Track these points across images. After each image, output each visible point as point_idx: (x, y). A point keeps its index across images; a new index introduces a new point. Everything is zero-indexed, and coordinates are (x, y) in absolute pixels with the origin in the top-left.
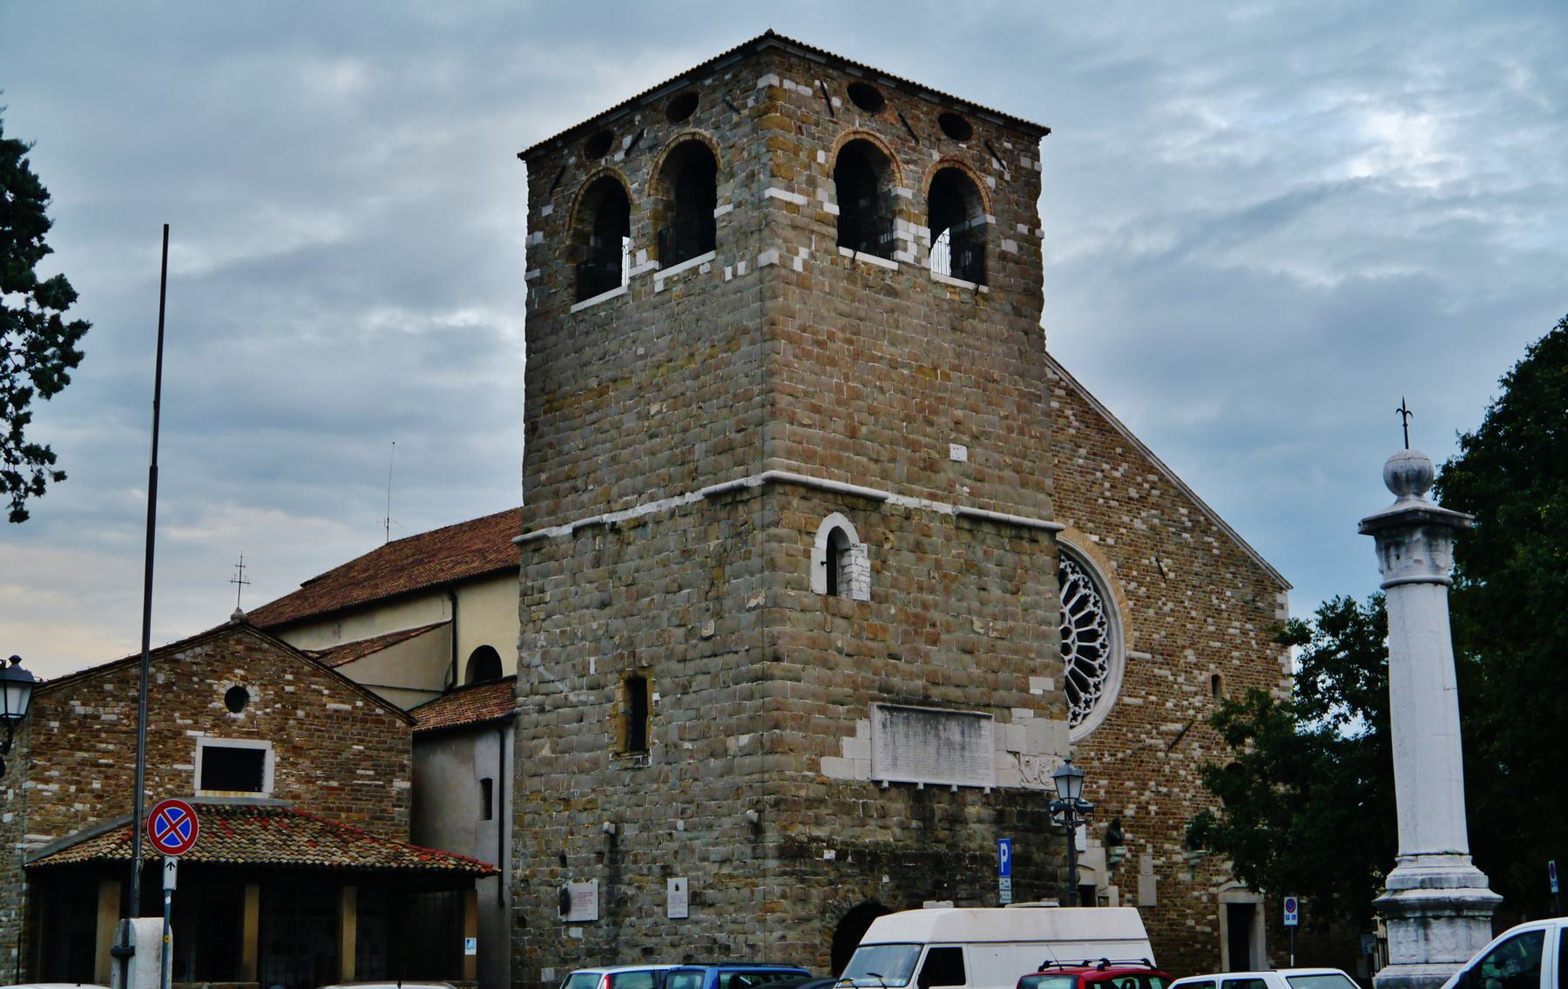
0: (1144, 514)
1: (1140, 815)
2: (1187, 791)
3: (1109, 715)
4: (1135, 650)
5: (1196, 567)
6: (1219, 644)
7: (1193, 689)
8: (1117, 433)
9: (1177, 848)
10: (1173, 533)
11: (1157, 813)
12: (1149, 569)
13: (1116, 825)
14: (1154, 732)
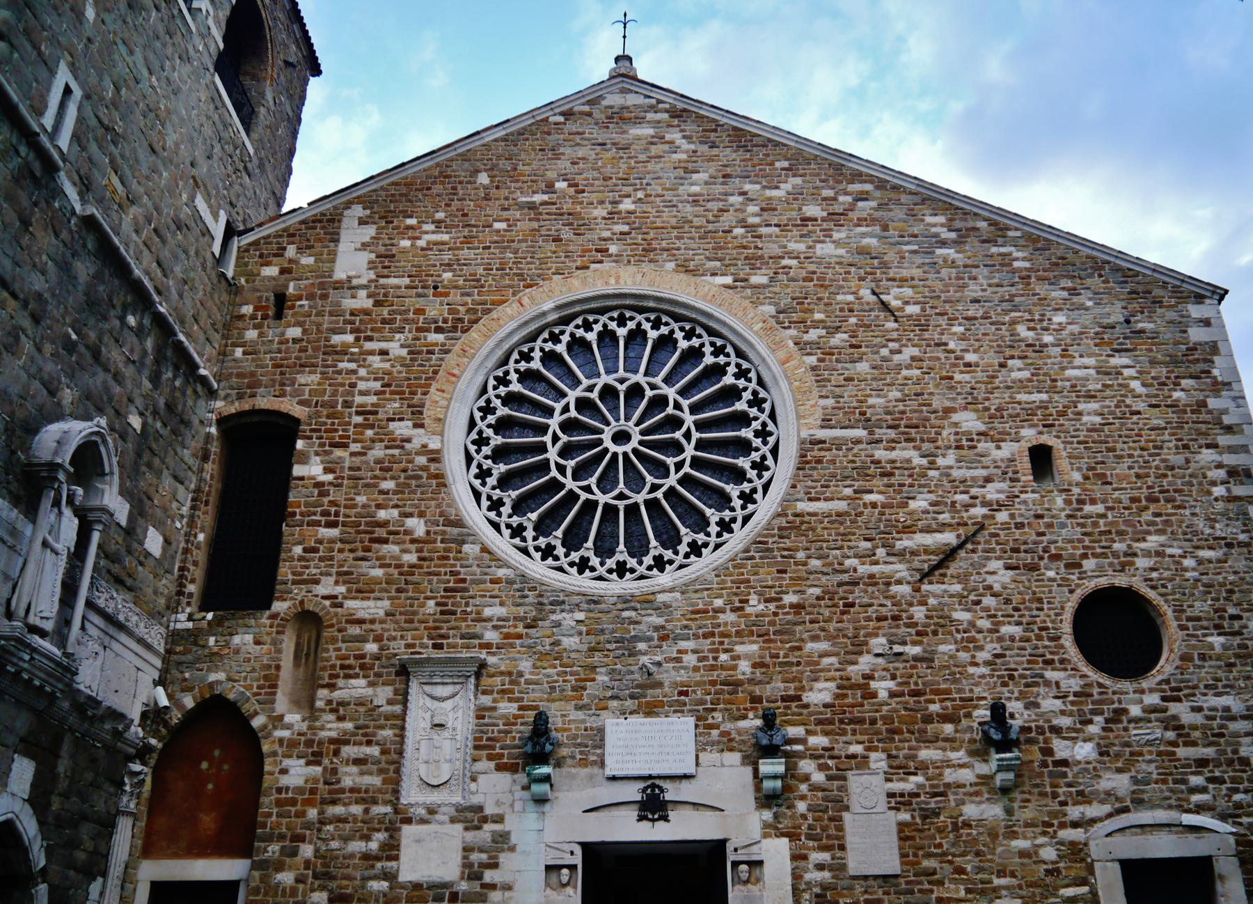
0: (836, 236)
1: (850, 700)
2: (981, 648)
3: (760, 535)
4: (823, 427)
5: (973, 290)
6: (1044, 397)
7: (984, 473)
8: (777, 144)
9: (959, 756)
10: (915, 252)
11: (893, 694)
12: (856, 307)
13: (769, 721)
14: (881, 552)
